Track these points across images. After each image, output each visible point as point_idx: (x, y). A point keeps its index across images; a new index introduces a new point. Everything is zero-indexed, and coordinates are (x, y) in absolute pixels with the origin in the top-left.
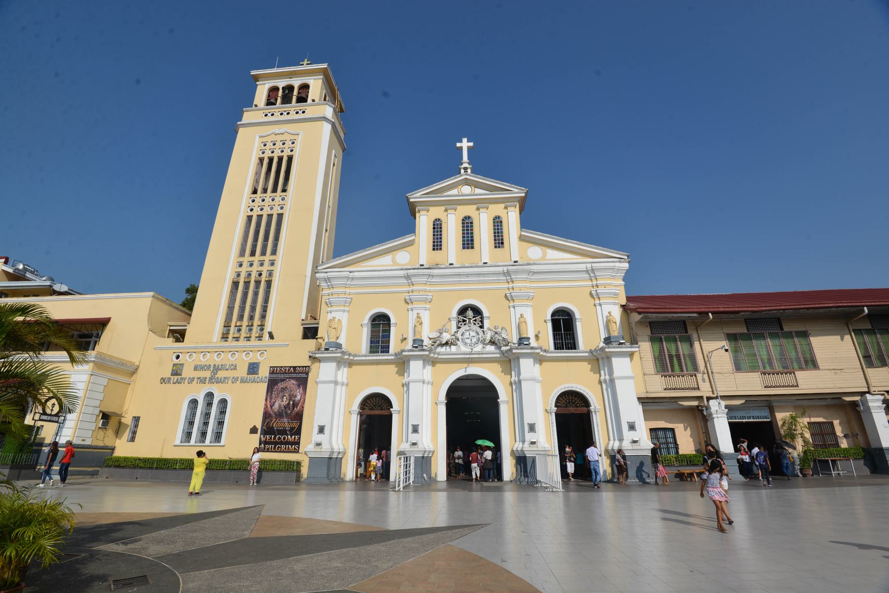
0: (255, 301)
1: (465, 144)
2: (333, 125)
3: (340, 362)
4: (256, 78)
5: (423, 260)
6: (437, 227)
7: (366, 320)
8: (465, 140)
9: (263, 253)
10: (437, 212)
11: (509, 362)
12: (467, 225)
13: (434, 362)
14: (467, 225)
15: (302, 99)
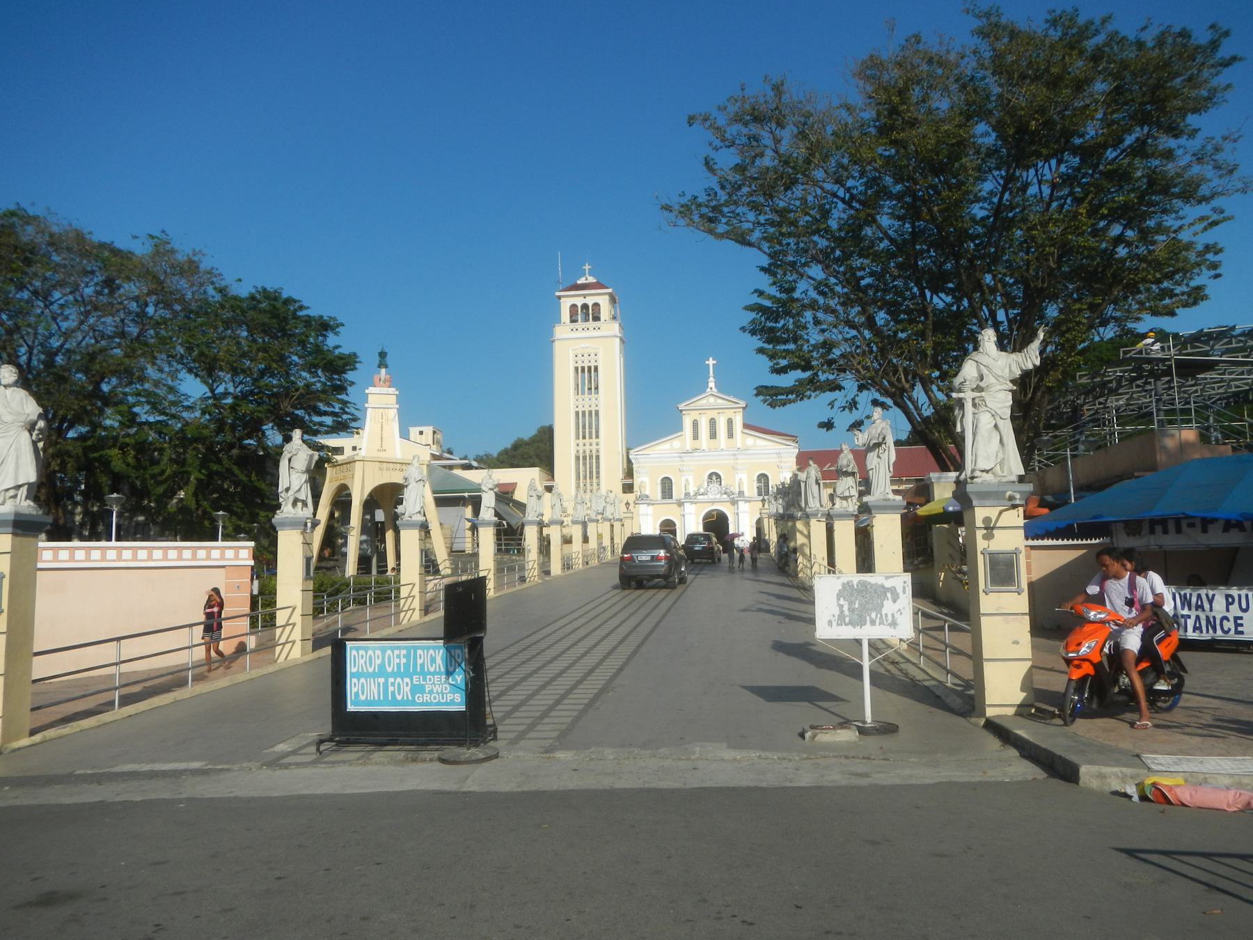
0: (591, 468)
1: (711, 362)
2: (621, 339)
3: (649, 504)
4: (559, 297)
5: (688, 447)
6: (695, 424)
7: (659, 481)
8: (711, 359)
9: (591, 437)
10: (695, 415)
11: (734, 502)
12: (713, 423)
13: (696, 503)
14: (713, 423)
15: (596, 318)
